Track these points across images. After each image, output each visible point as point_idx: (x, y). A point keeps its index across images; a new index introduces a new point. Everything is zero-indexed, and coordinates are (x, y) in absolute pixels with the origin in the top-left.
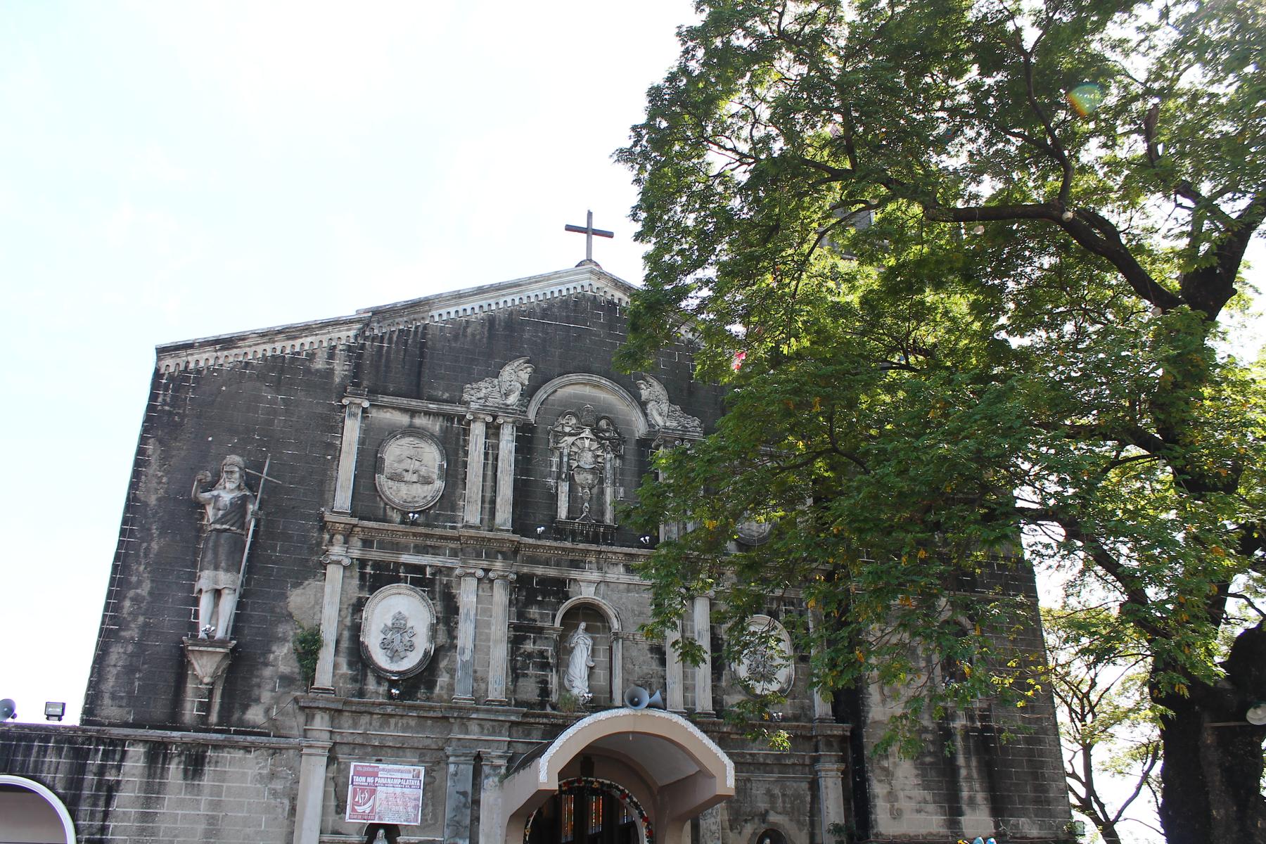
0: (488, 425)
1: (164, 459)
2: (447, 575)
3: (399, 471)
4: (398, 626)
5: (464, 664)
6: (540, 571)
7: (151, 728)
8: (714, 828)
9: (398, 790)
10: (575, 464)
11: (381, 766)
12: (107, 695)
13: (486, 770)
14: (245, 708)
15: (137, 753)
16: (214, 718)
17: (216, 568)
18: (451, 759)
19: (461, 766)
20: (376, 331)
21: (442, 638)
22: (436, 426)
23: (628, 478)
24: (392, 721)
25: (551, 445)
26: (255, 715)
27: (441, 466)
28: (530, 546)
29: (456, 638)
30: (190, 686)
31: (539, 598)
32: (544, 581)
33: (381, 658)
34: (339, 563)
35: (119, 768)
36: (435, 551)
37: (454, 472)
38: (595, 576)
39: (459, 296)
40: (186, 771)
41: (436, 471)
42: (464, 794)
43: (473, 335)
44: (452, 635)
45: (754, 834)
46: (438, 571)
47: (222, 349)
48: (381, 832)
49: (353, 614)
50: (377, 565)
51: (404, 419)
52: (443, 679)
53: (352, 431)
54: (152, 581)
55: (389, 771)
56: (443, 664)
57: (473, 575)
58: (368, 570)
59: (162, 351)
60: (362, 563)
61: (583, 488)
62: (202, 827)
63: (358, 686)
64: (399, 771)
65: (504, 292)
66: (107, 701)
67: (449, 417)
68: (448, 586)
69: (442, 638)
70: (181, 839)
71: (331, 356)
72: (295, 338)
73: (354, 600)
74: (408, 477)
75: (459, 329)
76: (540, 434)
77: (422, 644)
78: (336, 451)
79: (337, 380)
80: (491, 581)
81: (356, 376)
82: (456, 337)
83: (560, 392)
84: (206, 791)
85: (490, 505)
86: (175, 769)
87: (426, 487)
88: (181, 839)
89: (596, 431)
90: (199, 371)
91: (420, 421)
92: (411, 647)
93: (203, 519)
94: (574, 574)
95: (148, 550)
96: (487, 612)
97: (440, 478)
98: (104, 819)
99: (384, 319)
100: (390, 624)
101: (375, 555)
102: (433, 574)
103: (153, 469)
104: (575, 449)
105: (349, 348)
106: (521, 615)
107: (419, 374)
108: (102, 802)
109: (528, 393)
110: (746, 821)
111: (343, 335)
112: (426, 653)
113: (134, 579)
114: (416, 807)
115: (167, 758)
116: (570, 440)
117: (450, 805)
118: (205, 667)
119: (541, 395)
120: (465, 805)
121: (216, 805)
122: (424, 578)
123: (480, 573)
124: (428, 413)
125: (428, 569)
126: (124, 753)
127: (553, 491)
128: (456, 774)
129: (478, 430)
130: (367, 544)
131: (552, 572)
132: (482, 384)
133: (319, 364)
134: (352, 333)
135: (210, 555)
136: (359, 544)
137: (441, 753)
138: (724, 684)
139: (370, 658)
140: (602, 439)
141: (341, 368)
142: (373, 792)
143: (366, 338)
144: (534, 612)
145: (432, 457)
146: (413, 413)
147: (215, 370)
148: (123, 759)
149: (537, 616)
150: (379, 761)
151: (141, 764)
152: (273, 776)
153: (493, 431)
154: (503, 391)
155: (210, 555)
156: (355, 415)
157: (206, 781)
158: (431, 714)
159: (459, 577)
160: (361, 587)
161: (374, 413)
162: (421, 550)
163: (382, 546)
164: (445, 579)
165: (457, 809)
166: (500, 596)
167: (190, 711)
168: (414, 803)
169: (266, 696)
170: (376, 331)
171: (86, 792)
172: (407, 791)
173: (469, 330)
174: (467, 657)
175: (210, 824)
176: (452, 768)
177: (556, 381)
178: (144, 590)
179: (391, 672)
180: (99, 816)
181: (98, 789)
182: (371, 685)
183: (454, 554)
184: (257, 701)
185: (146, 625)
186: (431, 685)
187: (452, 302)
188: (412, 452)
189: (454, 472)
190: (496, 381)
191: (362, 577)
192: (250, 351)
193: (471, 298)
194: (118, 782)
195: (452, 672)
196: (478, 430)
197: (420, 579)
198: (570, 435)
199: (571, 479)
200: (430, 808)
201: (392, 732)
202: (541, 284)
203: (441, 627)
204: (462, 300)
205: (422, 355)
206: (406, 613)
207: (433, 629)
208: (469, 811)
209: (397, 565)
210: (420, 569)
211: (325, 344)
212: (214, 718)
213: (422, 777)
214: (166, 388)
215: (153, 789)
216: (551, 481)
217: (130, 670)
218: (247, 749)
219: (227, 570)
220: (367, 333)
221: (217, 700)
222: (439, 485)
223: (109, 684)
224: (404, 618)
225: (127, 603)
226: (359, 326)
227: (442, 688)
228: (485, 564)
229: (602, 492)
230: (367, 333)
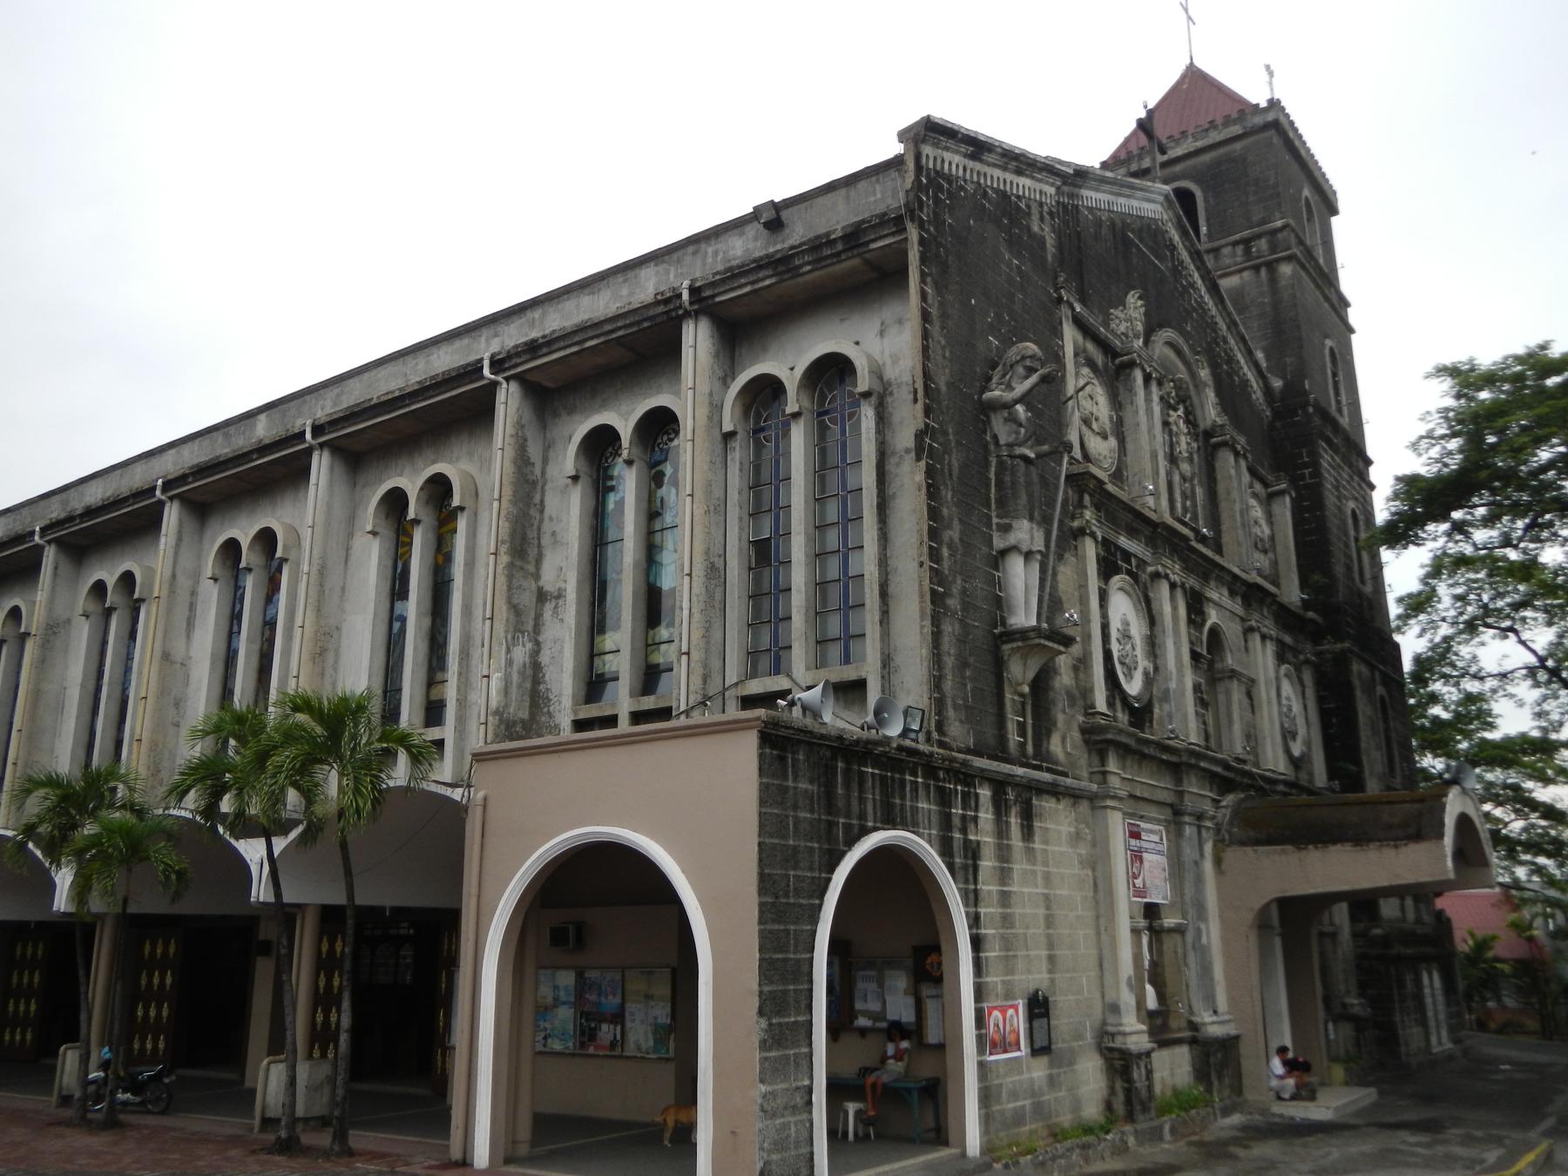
1: (944, 316)
7: (991, 757)
11: (1142, 825)
12: (949, 702)
13: (1204, 832)
14: (1049, 736)
15: (985, 793)
16: (1030, 749)
17: (1031, 519)
18: (1187, 819)
26: (1055, 746)
27: (1111, 418)
30: (1008, 696)
34: (1093, 535)
35: (975, 819)
40: (1022, 825)
46: (1142, 563)
47: (974, 157)
54: (961, 521)
59: (930, 131)
62: (1042, 911)
66: (951, 713)
70: (1032, 931)
71: (1042, 219)
72: (1019, 172)
74: (1095, 426)
79: (1050, 258)
84: (1039, 857)
86: (1014, 821)
88: (1032, 931)
89: (1188, 413)
90: (949, 178)
93: (985, 432)
95: (950, 465)
98: (976, 905)
103: (935, 329)
108: (971, 877)
112: (1146, 674)
113: (945, 511)
115: (1008, 808)
118: (1020, 672)
121: (1047, 877)
126: (977, 795)
129: (1138, 376)
131: (1197, 586)
135: (1023, 499)
142: (1141, 860)
147: (962, 188)
148: (977, 809)
150: (1142, 817)
151: (990, 816)
152: (1077, 837)
155: (1023, 499)
157: (1037, 845)
162: (1132, 533)
167: (1014, 738)
169: (1060, 718)
171: (958, 860)
175: (1048, 908)
178: (953, 533)
180: (972, 896)
181: (966, 857)
182: (1120, 715)
184: (1055, 724)
185: (964, 592)
192: (986, 169)
194: (978, 843)
196: (1138, 376)
209: (1118, 548)
212: (1030, 749)
214: (927, 187)
215: (1004, 854)
217: (963, 664)
218: (1054, 791)
219: (1039, 524)
221: (1030, 721)
222: (1113, 442)
223: (948, 685)
225: (945, 552)
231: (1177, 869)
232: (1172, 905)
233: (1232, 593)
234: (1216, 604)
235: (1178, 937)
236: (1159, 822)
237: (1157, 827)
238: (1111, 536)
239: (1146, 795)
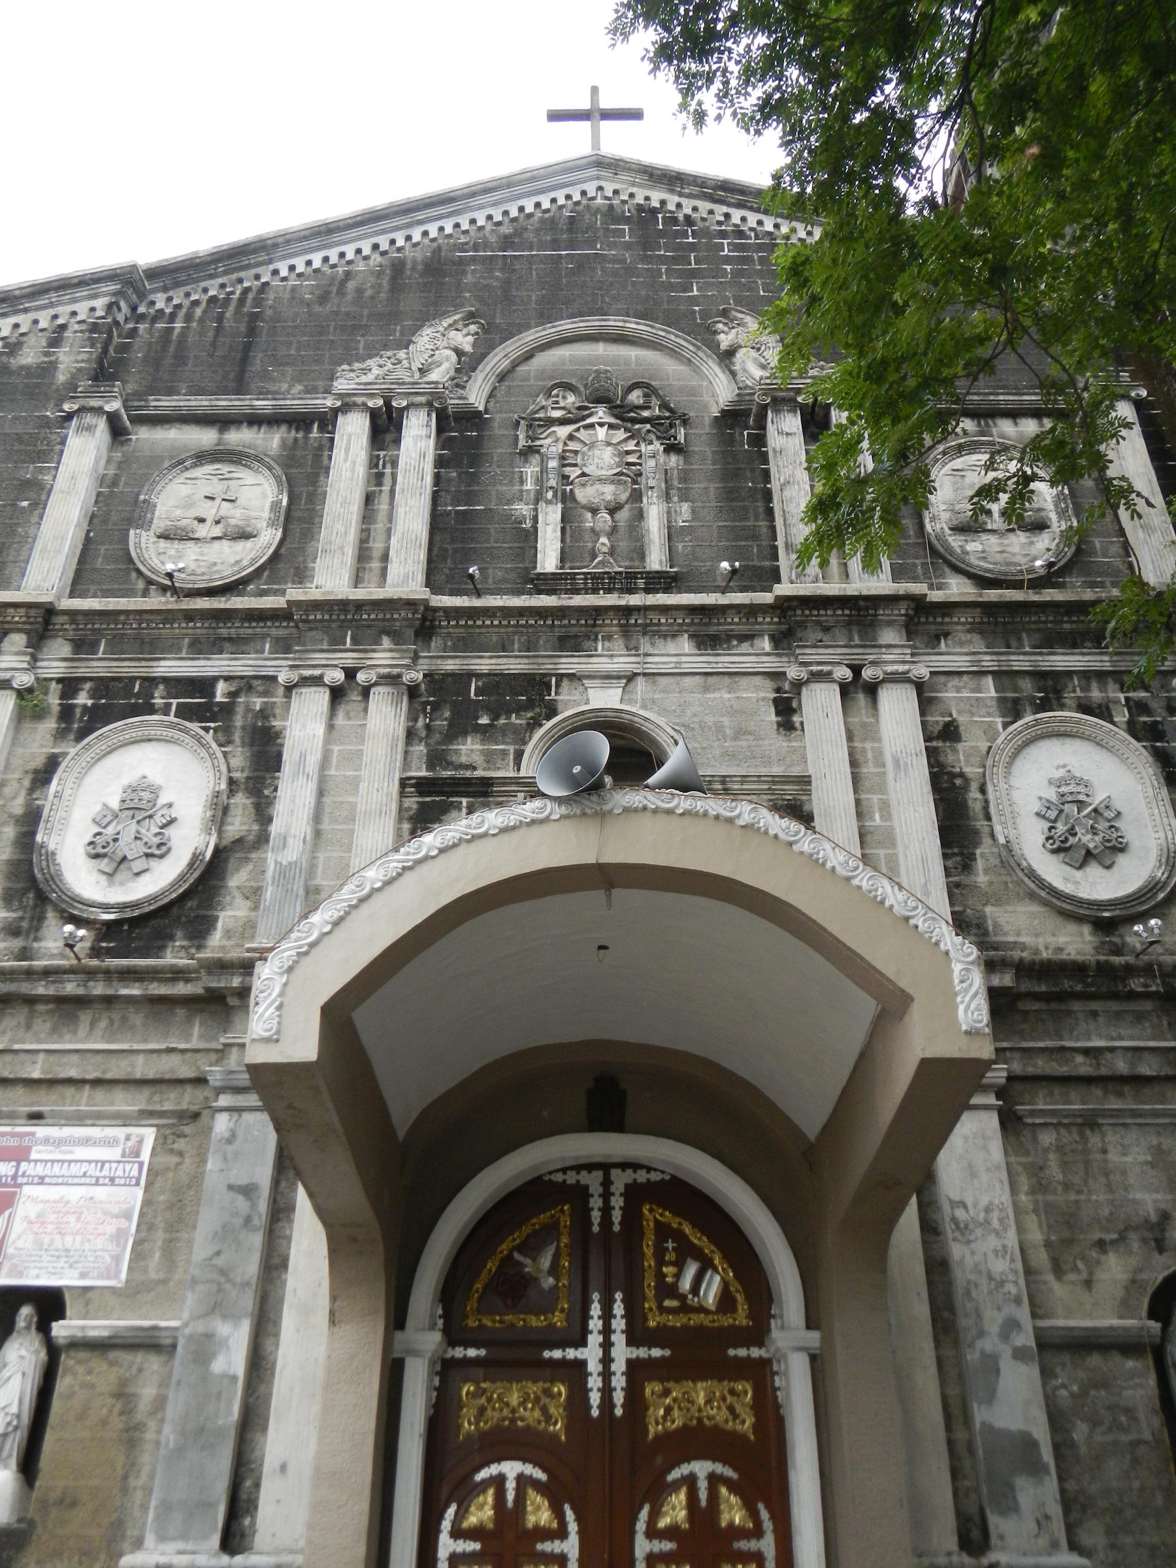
0: (374, 414)
2: (265, 694)
3: (184, 523)
4: (140, 804)
5: (284, 872)
6: (484, 664)
8: (999, 1266)
9: (75, 1194)
10: (574, 473)
11: (41, 1131)
19: (248, 1117)
20: (160, 305)
21: (239, 824)
22: (273, 440)
23: (698, 486)
24: (85, 1017)
25: (522, 442)
27: (275, 506)
28: (459, 612)
29: (270, 820)
31: (484, 720)
32: (496, 683)
33: (83, 880)
36: (238, 645)
37: (300, 517)
38: (623, 663)
39: (326, 232)
41: (266, 514)
42: (248, 1191)
43: (360, 291)
44: (263, 813)
45: (1134, 1283)
46: (245, 684)
48: (26, 1312)
49: (31, 790)
50: (102, 686)
51: (206, 437)
52: (231, 914)
53: (83, 456)
55: (59, 1143)
56: (237, 879)
57: (317, 681)
58: (83, 699)
60: (70, 686)
61: (594, 511)
63: (17, 943)
64: (86, 1142)
65: (420, 216)
67: (300, 421)
68: (265, 713)
69: (239, 824)
73: (39, 762)
74: (202, 531)
75: (332, 285)
76: (498, 429)
77: (190, 840)
78: (37, 493)
80: (366, 692)
81: (104, 372)
82: (323, 298)
83: (543, 360)
85: (368, 556)
87: (241, 545)
91: (238, 437)
92: (159, 851)
94: (569, 664)
96: (354, 758)
97: (272, 524)
99: (177, 285)
100: (115, 804)
101: (99, 666)
102: (233, 695)
104: (573, 446)
105: (94, 328)
106: (435, 759)
107: (244, 361)
109: (467, 364)
110: (1101, 1245)
111: (82, 308)
112: (195, 857)
114: (120, 1235)
116: (563, 431)
117: (208, 1220)
119: (498, 360)
120: (248, 1220)
122: (210, 705)
123: (338, 676)
124: (255, 420)
125: (221, 688)
127: (528, 524)
128: (231, 1139)
130: (83, 646)
131: (514, 664)
132: (371, 362)
133: (29, 357)
134: (100, 303)
136: (66, 650)
137: (201, 1093)
138: (981, 878)
139: (54, 878)
140: (634, 421)
141: (71, 359)
143: (141, 318)
144: (469, 749)
145: (258, 495)
146: (223, 422)
149: (477, 759)
153: (385, 427)
154: (416, 365)
156: (90, 429)
158: (182, 989)
159: (289, 689)
160: (60, 735)
161: (143, 435)
162: (199, 648)
163: (117, 646)
164: (258, 702)
165: (225, 1233)
166: (385, 717)
168: (111, 1228)
170: (160, 305)
172: (101, 1193)
173: (351, 285)
174: (293, 852)
176: (222, 1124)
177: (531, 336)
179: (106, 907)
183: (284, 646)
186: (200, 929)
187: (314, 243)
188: (216, 488)
189: (300, 517)
190: (402, 354)
191: (66, 713)
193: (354, 233)
195: (254, 894)
197: (198, 703)
198: (563, 422)
199: (567, 499)
200: (160, 1235)
201: (87, 1043)
202: (497, 196)
203: (241, 801)
204: (336, 238)
205: (252, 331)
206: (156, 778)
207: (220, 812)
208: (257, 1240)
209: (150, 682)
210: (203, 686)
211: (43, 324)
213: (145, 1156)
216: (523, 509)
220: (142, 309)
224: (155, 791)
226: (113, 287)
227: (228, 934)
228: (349, 658)
229: (640, 515)
230: (142, 309)
231: (167, 1212)
232: (133, 1292)
233: (707, 642)
234: (608, 677)
235: (153, 1363)
236: (125, 1120)
237: (120, 1132)
238: (127, 668)
239: (73, 1073)
